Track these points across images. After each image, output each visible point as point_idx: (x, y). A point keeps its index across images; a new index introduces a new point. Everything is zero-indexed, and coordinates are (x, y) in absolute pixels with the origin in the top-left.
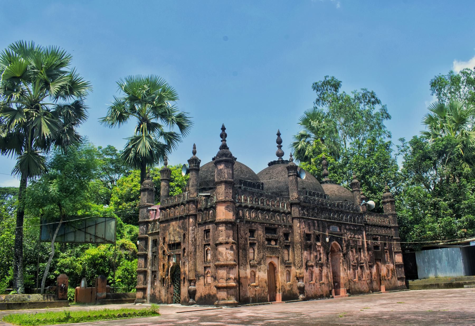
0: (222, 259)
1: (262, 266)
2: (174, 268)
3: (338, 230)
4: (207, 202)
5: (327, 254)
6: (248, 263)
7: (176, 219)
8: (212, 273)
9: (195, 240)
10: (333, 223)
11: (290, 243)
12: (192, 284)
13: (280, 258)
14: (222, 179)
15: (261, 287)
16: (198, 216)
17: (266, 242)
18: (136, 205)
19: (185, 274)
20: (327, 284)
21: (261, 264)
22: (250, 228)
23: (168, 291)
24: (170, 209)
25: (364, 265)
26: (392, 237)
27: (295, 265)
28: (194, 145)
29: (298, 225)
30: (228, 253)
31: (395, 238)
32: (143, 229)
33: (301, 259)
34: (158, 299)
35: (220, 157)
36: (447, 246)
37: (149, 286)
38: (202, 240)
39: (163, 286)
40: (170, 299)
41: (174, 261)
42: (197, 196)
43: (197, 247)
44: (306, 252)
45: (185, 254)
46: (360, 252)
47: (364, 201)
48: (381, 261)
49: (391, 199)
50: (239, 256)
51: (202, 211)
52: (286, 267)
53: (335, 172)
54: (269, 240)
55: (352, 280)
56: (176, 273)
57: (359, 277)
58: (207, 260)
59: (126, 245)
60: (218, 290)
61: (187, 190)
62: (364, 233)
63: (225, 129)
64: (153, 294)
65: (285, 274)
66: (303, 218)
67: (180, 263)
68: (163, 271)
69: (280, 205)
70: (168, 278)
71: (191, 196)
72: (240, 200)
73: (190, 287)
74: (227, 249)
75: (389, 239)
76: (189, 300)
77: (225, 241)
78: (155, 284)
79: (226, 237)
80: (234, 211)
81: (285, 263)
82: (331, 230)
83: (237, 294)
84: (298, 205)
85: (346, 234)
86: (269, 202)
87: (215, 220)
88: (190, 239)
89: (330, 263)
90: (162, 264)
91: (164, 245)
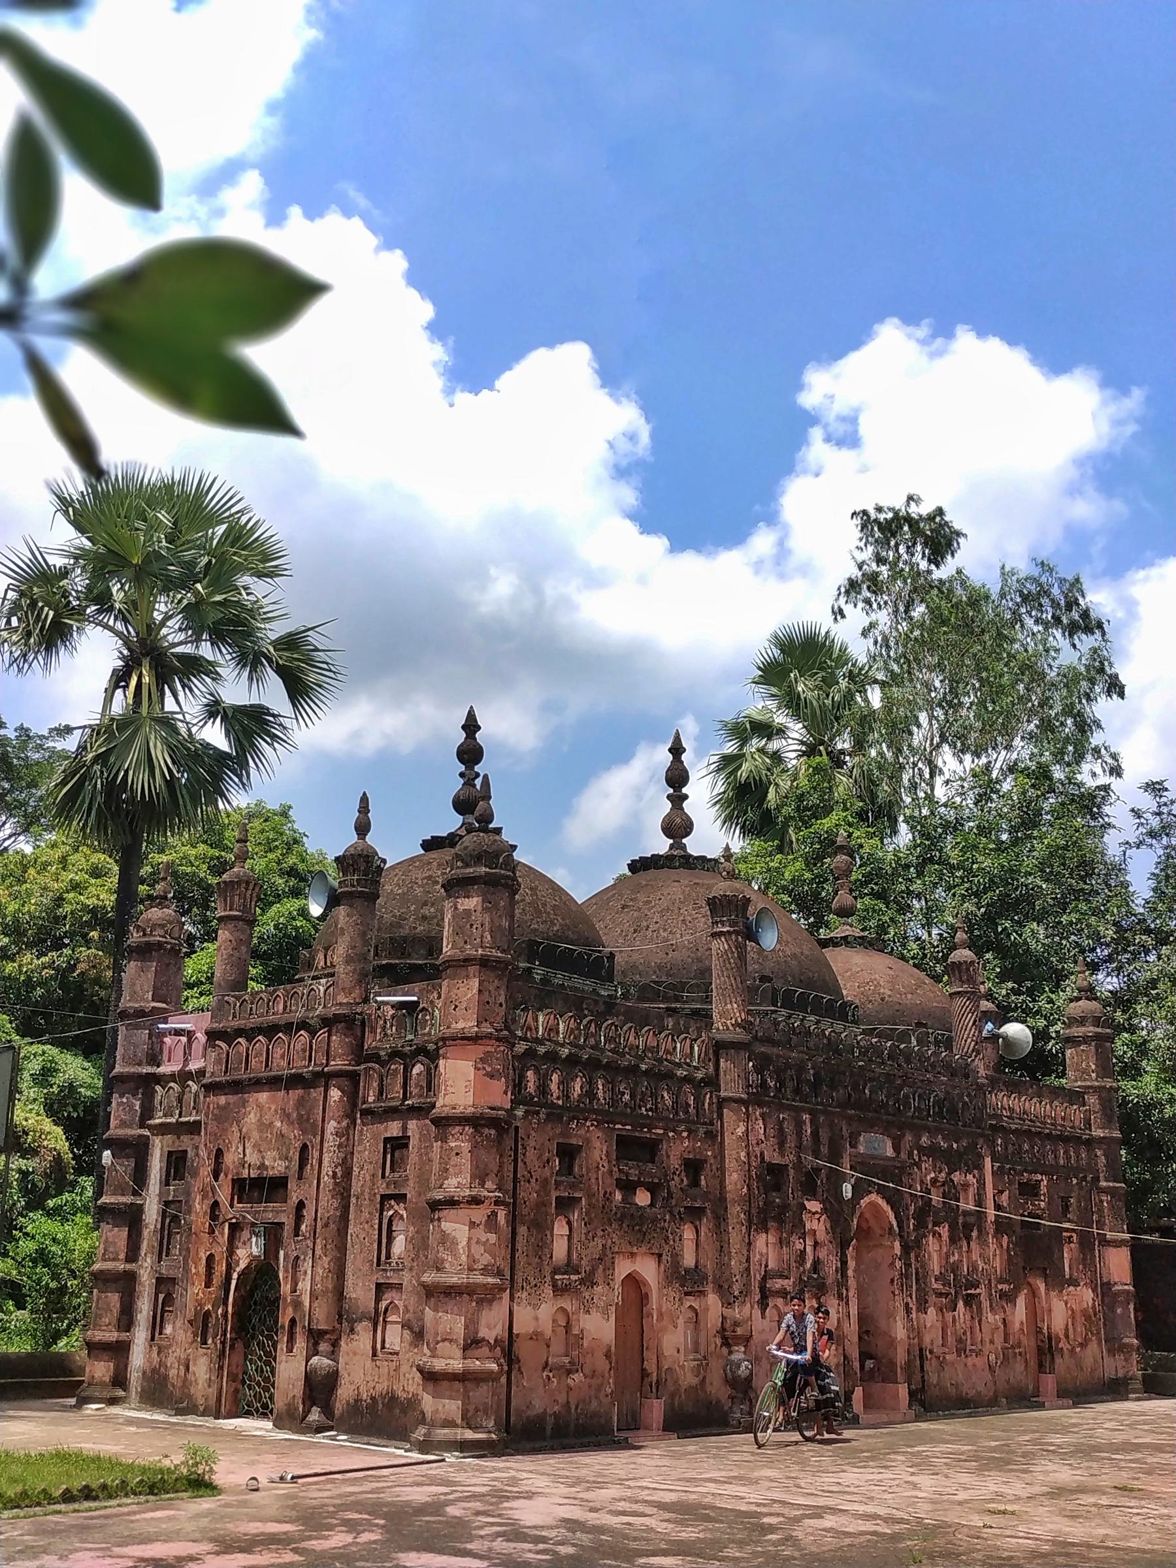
0: (452, 1264)
1: (598, 1289)
2: (253, 1276)
3: (890, 1152)
4: (401, 1026)
5: (843, 1245)
6: (548, 1279)
7: (274, 1083)
8: (407, 1310)
9: (348, 1173)
10: (870, 1126)
11: (706, 1196)
12: (323, 1347)
13: (664, 1257)
14: (470, 951)
15: (590, 1374)
17: (618, 1196)
18: (75, 965)
19: (297, 1304)
20: (837, 1365)
21: (593, 1284)
22: (561, 1140)
23: (221, 1368)
24: (249, 1040)
25: (981, 1290)
26: (1096, 1179)
27: (721, 1287)
28: (364, 800)
29: (740, 1130)
30: (478, 1242)
31: (1103, 1184)
32: (131, 1107)
33: (746, 1265)
34: (178, 1393)
35: (467, 865)
37: (140, 1335)
39: (204, 1342)
40: (229, 1397)
41: (255, 1251)
42: (366, 1000)
43: (353, 1200)
44: (764, 1235)
45: (303, 1227)
46: (969, 1239)
47: (990, 1026)
48: (1046, 1277)
49: (1099, 1030)
50: (513, 1251)
51: (383, 1064)
52: (687, 1294)
53: (880, 896)
54: (629, 1187)
55: (931, 1352)
56: (258, 1296)
57: (960, 1341)
58: (388, 1256)
59: (27, 1134)
60: (430, 1386)
61: (322, 963)
62: (988, 1161)
63: (479, 728)
64: (154, 1371)
65: (680, 1322)
66: (760, 1105)
67: (277, 1259)
68: (208, 1284)
69: (675, 1048)
70: (225, 1315)
71: (342, 999)
72: (529, 1028)
73: (315, 1360)
74: (472, 1225)
75: (1081, 1188)
76: (307, 1412)
77: (468, 1192)
78: (168, 1330)
79: (473, 1177)
80: (507, 1077)
81: (682, 1280)
82: (861, 1149)
83: (499, 1400)
84: (742, 1053)
85: (920, 1168)
86: (637, 1036)
87: (433, 1106)
88: (327, 1168)
89: (852, 1283)
90: (203, 1256)
91: (216, 1178)
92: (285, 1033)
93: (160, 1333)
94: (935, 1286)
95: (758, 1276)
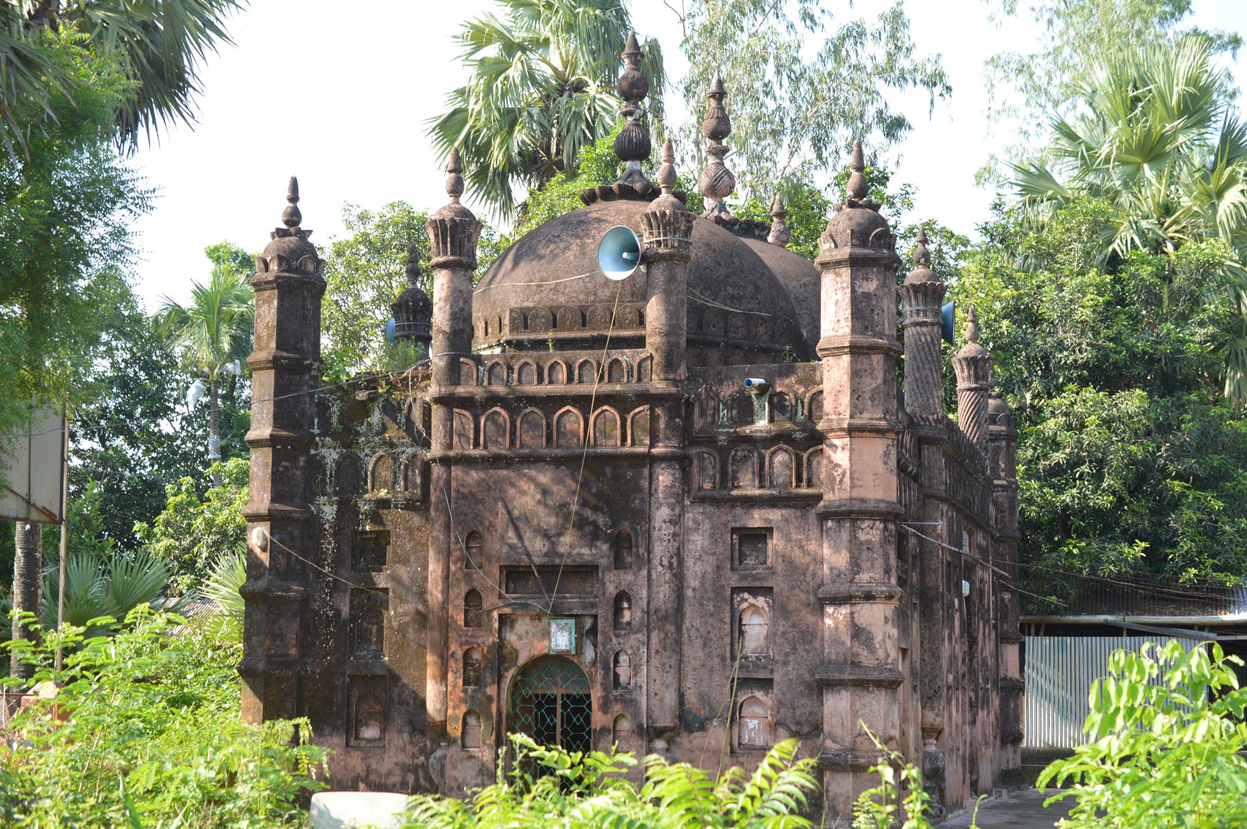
9: (681, 562)
16: (695, 462)
36: (1164, 630)
38: (718, 567)
87: (819, 497)
92: (573, 406)
93: (357, 738)
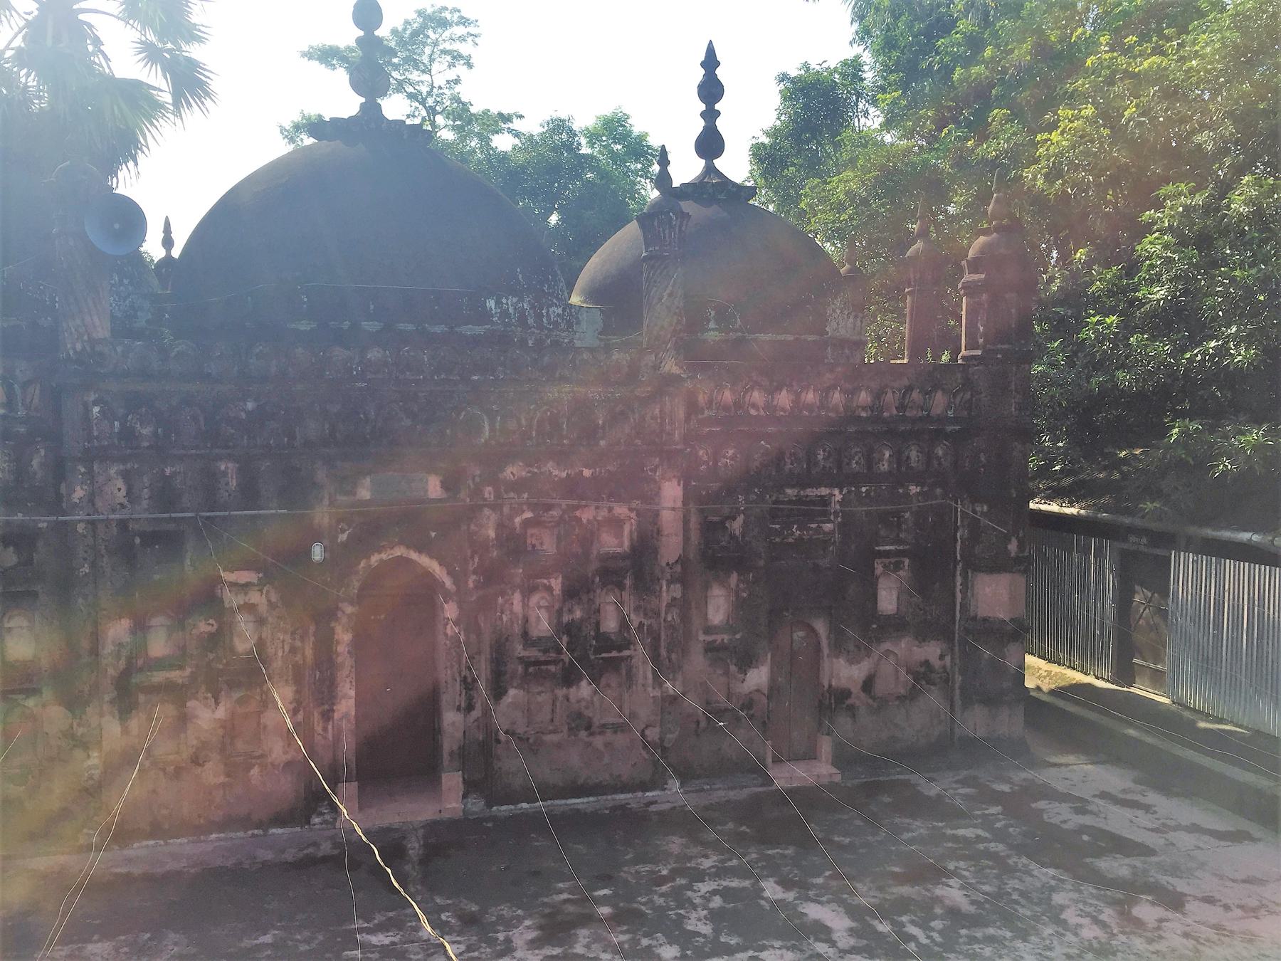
25: (639, 652)
29: (79, 493)
82: (364, 493)
94: (526, 654)
95: (111, 671)
